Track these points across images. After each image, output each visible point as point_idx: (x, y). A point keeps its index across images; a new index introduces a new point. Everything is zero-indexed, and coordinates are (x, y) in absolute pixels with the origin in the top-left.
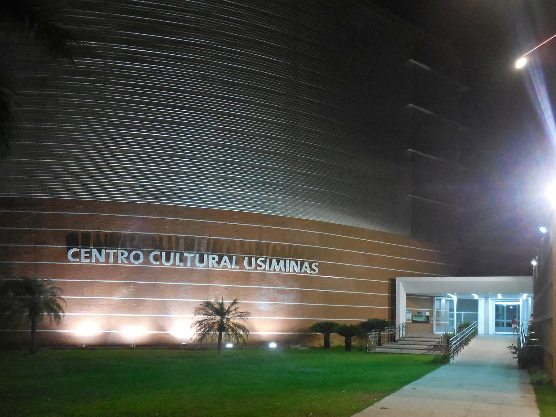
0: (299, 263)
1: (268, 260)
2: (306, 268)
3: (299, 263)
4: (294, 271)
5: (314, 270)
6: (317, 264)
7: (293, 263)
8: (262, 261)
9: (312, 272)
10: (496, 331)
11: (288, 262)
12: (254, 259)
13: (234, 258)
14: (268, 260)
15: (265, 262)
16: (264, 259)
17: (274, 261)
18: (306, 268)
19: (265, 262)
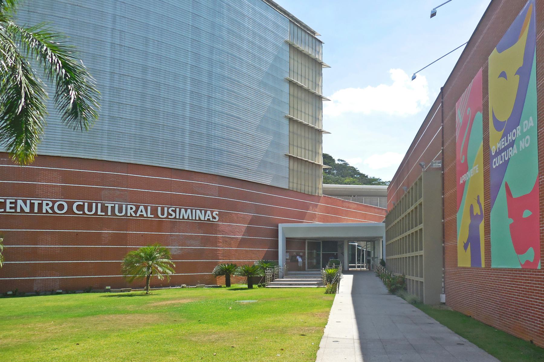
0: (203, 212)
1: (178, 210)
2: (142, 212)
3: (203, 212)
4: (200, 219)
5: (215, 218)
6: (217, 213)
7: (198, 211)
8: (172, 210)
9: (214, 220)
10: (289, 241)
11: (194, 211)
12: (166, 209)
13: (149, 208)
14: (178, 210)
15: (175, 211)
16: (174, 209)
17: (183, 211)
18: (142, 212)
19: (175, 211)
